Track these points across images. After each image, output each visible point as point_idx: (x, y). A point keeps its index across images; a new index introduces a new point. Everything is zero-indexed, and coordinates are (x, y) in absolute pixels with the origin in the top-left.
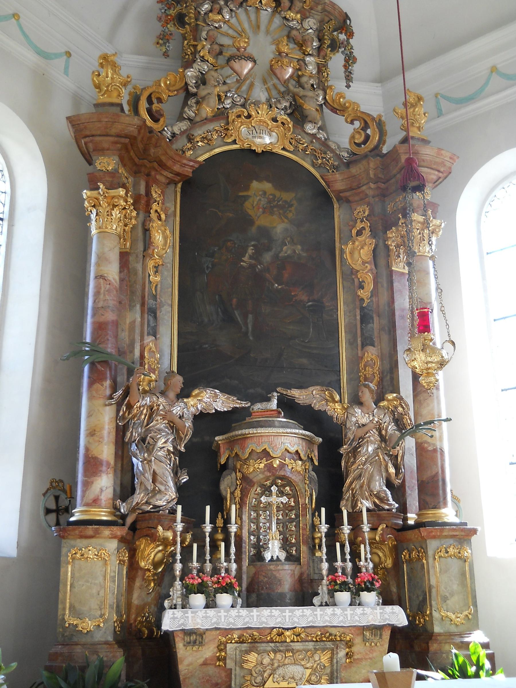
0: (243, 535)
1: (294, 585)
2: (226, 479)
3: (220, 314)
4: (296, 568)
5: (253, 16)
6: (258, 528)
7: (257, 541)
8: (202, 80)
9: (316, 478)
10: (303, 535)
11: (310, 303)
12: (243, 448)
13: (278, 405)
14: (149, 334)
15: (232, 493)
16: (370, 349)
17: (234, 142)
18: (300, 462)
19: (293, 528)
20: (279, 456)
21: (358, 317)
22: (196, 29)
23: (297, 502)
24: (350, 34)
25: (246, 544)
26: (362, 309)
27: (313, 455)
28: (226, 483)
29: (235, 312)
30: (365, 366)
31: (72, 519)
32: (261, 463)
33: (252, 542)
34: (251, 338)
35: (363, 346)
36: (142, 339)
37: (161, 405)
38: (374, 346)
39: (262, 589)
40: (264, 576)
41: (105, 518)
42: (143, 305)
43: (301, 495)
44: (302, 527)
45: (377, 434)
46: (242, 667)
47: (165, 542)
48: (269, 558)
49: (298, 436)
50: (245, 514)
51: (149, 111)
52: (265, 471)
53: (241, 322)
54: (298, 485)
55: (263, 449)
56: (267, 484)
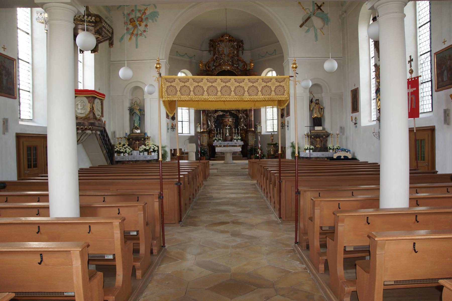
5: (225, 44)
8: (217, 57)
17: (222, 69)
22: (215, 48)
24: (243, 44)
47: (214, 133)
51: (208, 66)
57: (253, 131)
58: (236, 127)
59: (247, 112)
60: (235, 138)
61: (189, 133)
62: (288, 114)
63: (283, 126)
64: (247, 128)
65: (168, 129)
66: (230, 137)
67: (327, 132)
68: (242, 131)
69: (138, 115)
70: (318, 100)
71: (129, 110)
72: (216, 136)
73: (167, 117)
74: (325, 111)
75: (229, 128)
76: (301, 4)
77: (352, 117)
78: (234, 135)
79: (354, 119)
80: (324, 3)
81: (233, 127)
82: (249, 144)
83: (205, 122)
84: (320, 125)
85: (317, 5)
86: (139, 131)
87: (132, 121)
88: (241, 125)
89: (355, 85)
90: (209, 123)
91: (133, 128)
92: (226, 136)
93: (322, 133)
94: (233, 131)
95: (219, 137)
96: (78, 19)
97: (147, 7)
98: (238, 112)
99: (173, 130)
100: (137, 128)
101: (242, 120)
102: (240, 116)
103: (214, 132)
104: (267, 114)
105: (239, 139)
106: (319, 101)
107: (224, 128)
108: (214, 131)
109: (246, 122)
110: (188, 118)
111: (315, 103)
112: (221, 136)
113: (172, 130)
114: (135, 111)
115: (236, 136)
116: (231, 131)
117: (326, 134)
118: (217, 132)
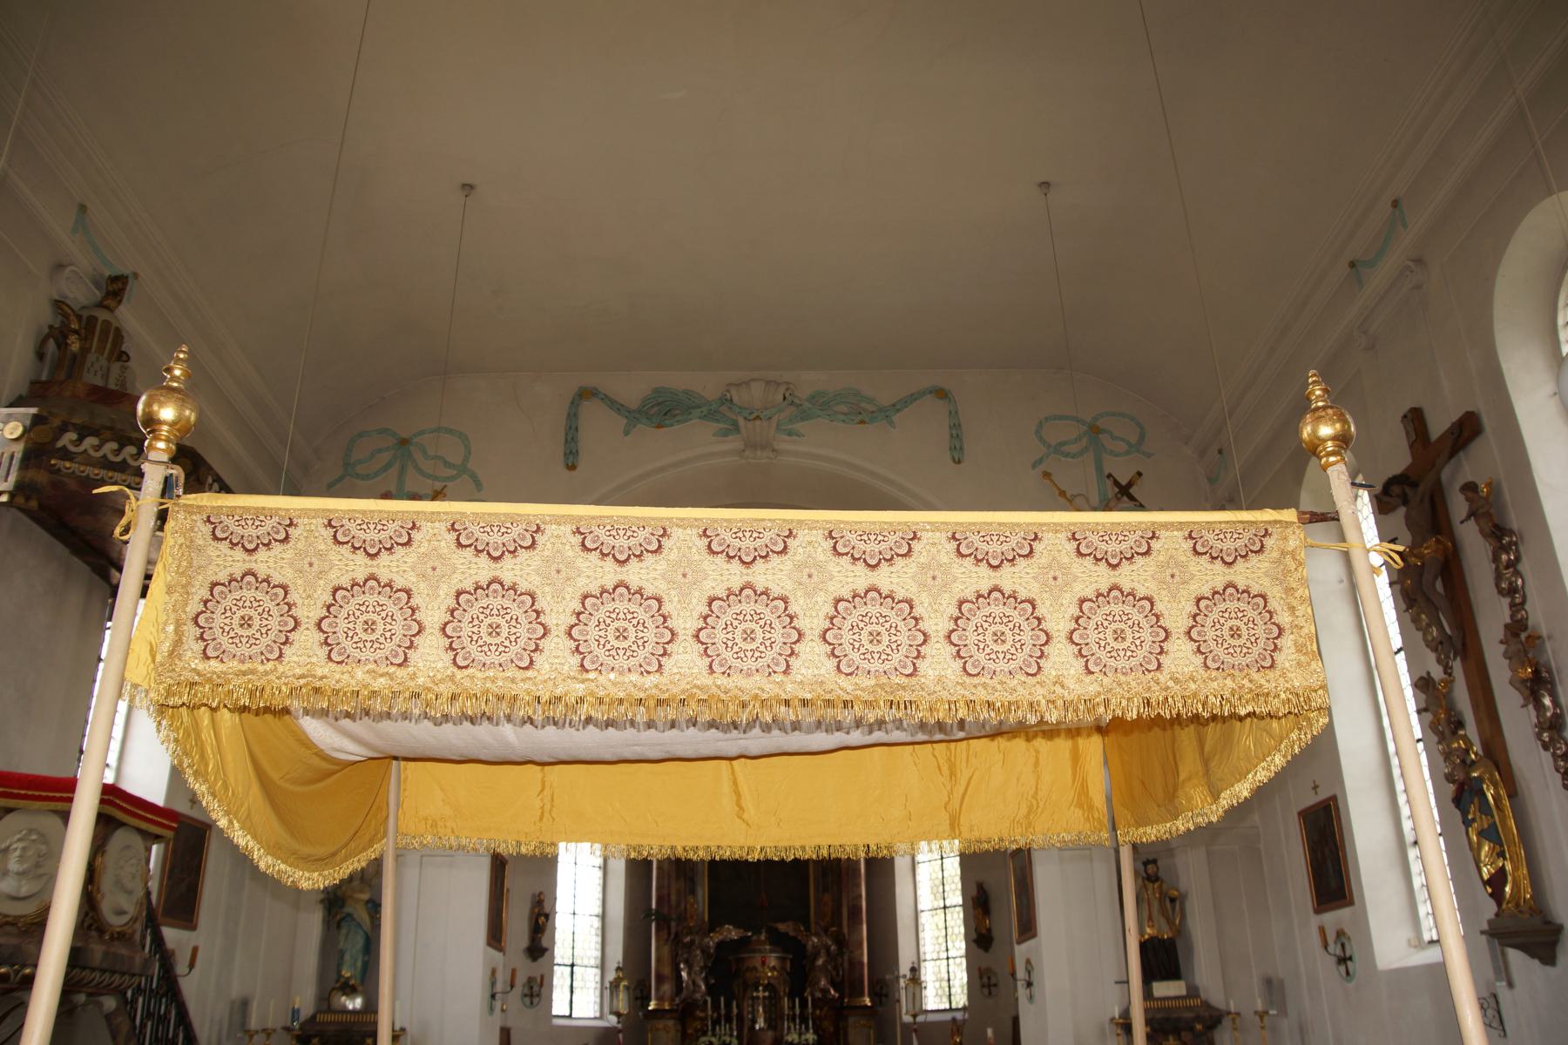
6: (754, 1010)
13: (766, 938)
15: (739, 990)
31: (650, 1008)
41: (667, 1008)
47: (704, 1019)
57: (866, 1006)
58: (796, 991)
59: (840, 926)
61: (598, 1015)
62: (1028, 929)
63: (993, 982)
64: (842, 997)
65: (493, 996)
66: (770, 1034)
67: (1207, 1005)
68: (821, 1009)
69: (362, 929)
70: (1154, 862)
71: (322, 901)
72: (714, 1029)
73: (492, 942)
74: (1188, 910)
75: (767, 994)
76: (1053, 478)
77: (1322, 930)
78: (789, 1028)
79: (1331, 938)
80: (1140, 474)
81: (783, 989)
83: (667, 971)
84: (1173, 973)
85: (1116, 483)
86: (356, 1003)
87: (330, 952)
88: (818, 982)
89: (1315, 788)
90: (684, 974)
91: (334, 989)
93: (1190, 1008)
94: (782, 1008)
95: (725, 1035)
96: (89, 455)
97: (445, 486)
98: (802, 928)
99: (532, 1003)
100: (349, 989)
101: (820, 962)
102: (814, 947)
103: (702, 1015)
104: (921, 935)
106: (1158, 868)
108: (704, 1009)
109: (836, 968)
110: (599, 954)
111: (1143, 878)
112: (731, 1029)
113: (527, 1000)
114: (347, 909)
117: (1207, 1014)
118: (715, 1015)
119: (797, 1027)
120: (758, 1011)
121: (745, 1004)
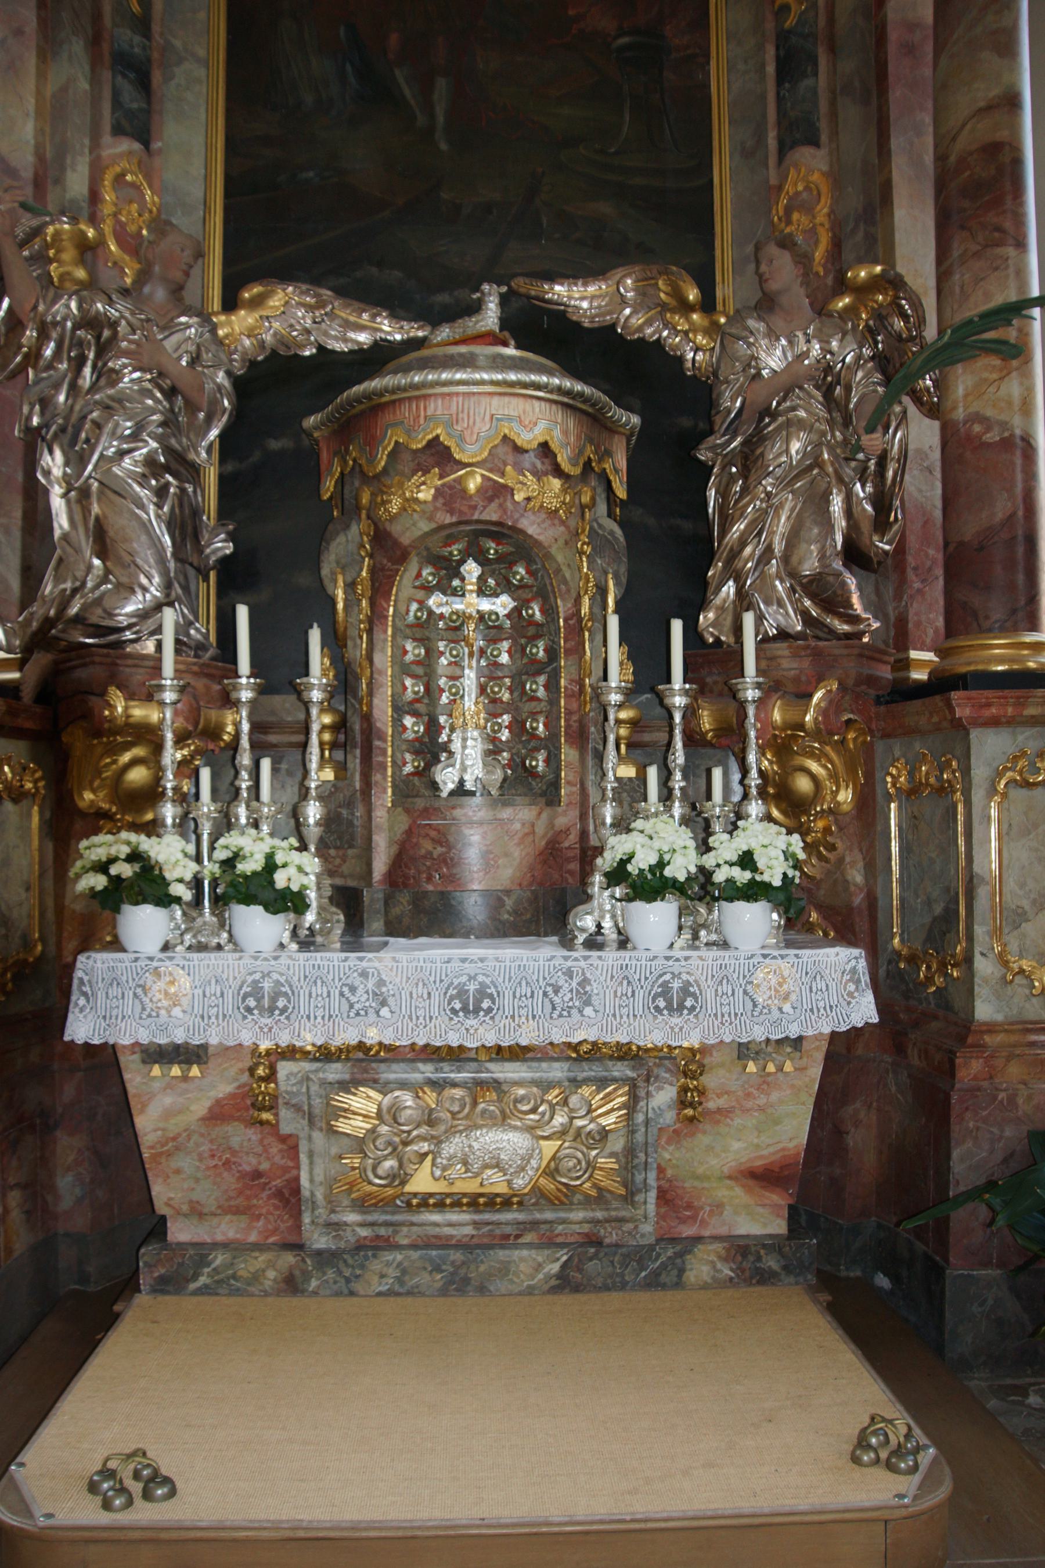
0: (376, 713)
1: (531, 869)
2: (333, 546)
3: (352, 79)
4: (540, 814)
6: (431, 692)
7: (427, 730)
9: (622, 539)
10: (569, 713)
11: (625, 40)
12: (372, 442)
14: (118, 131)
15: (350, 586)
16: (805, 154)
18: (556, 483)
19: (541, 693)
20: (479, 459)
21: (771, 69)
23: (550, 611)
25: (385, 741)
26: (782, 37)
27: (607, 466)
28: (332, 557)
29: (397, 72)
30: (788, 211)
32: (424, 483)
33: (410, 735)
34: (444, 146)
35: (783, 151)
36: (95, 144)
37: (123, 322)
38: (816, 143)
39: (430, 879)
40: (433, 840)
42: (95, 41)
43: (563, 587)
44: (566, 688)
45: (821, 399)
46: (332, 1131)
48: (451, 786)
49: (548, 396)
50: (383, 650)
52: (436, 509)
53: (412, 102)
54: (548, 556)
55: (430, 437)
56: (451, 553)
60: (644, 860)
78: (634, 790)
82: (984, 1010)
92: (434, 786)
98: (693, 295)
105: (754, 891)
107: (376, 618)
115: (667, 796)
116: (538, 686)
119: (678, 781)
120: (457, 697)
121: (383, 659)
